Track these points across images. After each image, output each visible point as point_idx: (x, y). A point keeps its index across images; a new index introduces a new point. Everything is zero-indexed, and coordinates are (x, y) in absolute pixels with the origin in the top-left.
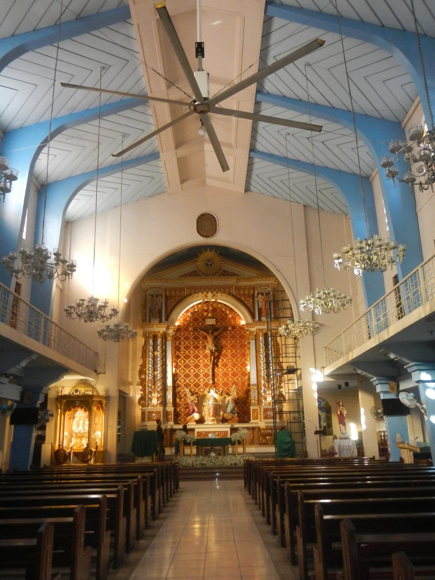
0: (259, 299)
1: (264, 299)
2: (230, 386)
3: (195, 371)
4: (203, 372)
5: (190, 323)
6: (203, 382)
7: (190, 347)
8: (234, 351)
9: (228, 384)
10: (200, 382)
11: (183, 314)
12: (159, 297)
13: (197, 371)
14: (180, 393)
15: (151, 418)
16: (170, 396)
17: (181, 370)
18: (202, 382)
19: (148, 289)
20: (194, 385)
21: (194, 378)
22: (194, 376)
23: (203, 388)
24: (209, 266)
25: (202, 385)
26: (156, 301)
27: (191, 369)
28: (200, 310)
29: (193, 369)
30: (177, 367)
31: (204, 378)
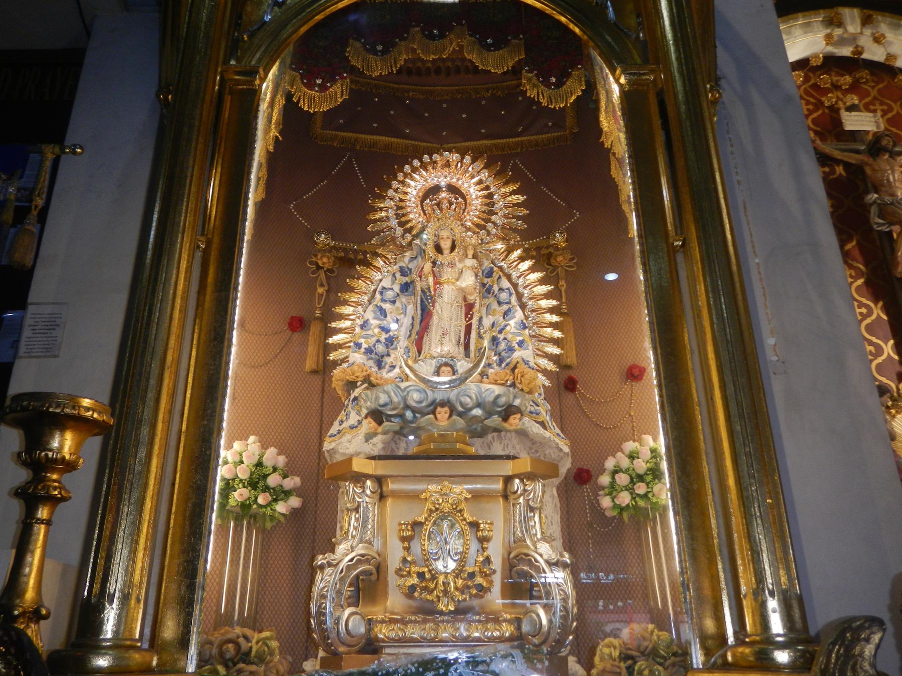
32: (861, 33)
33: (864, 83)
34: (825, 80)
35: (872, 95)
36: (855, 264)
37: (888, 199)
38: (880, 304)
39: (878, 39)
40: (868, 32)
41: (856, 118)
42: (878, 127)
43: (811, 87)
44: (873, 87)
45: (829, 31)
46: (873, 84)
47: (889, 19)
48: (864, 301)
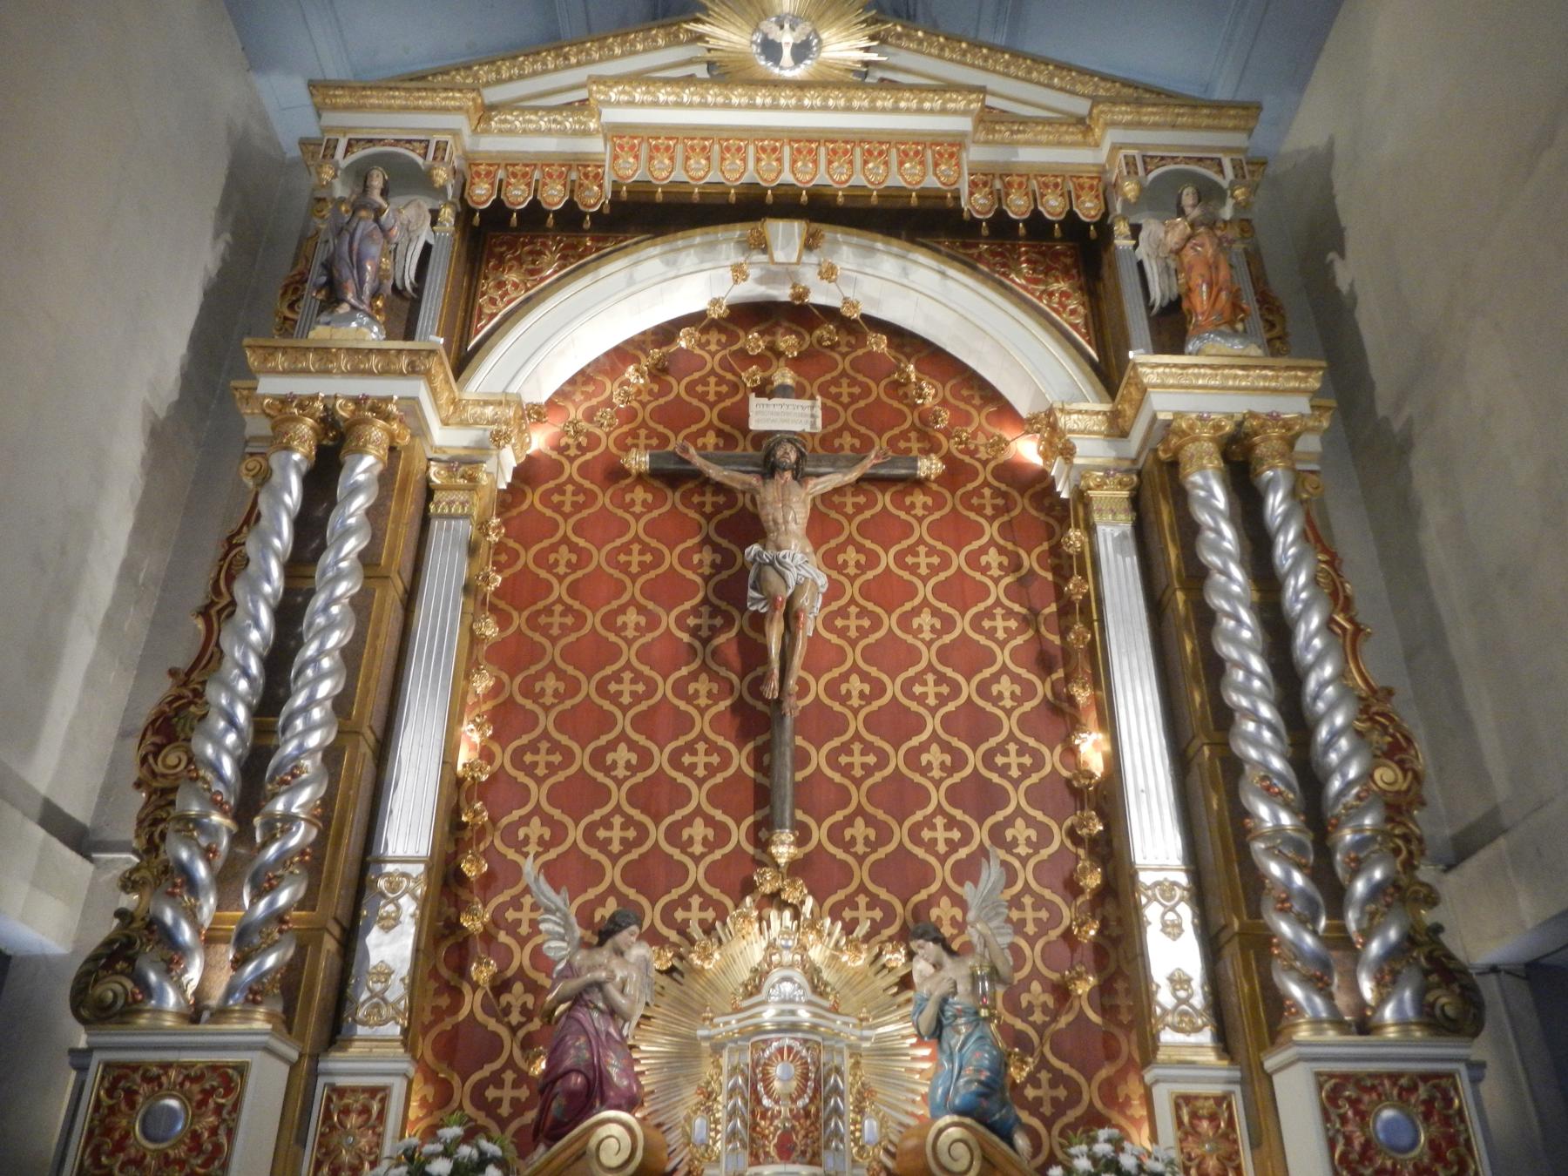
0: (1142, 253)
1: (1192, 225)
2: (945, 889)
3: (645, 758)
4: (711, 770)
5: (634, 434)
6: (710, 846)
7: (620, 588)
8: (963, 624)
9: (926, 876)
10: (685, 846)
11: (583, 378)
12: (408, 214)
13: (661, 759)
14: (503, 937)
15: (120, 1146)
16: (391, 948)
17: (533, 747)
18: (698, 849)
19: (332, 146)
20: (633, 875)
21: (636, 814)
22: (632, 796)
23: (708, 902)
24: (787, 52)
25: (696, 873)
26: (379, 212)
27: (612, 746)
28: (712, 363)
29: (632, 746)
30: (505, 719)
31: (718, 815)
32: (798, 262)
33: (832, 347)
34: (754, 341)
35: (840, 367)
36: (723, 672)
37: (767, 555)
38: (750, 746)
39: (828, 273)
40: (812, 258)
41: (777, 409)
42: (813, 425)
43: (733, 354)
44: (844, 355)
45: (741, 259)
46: (844, 349)
47: (855, 240)
48: (721, 741)
